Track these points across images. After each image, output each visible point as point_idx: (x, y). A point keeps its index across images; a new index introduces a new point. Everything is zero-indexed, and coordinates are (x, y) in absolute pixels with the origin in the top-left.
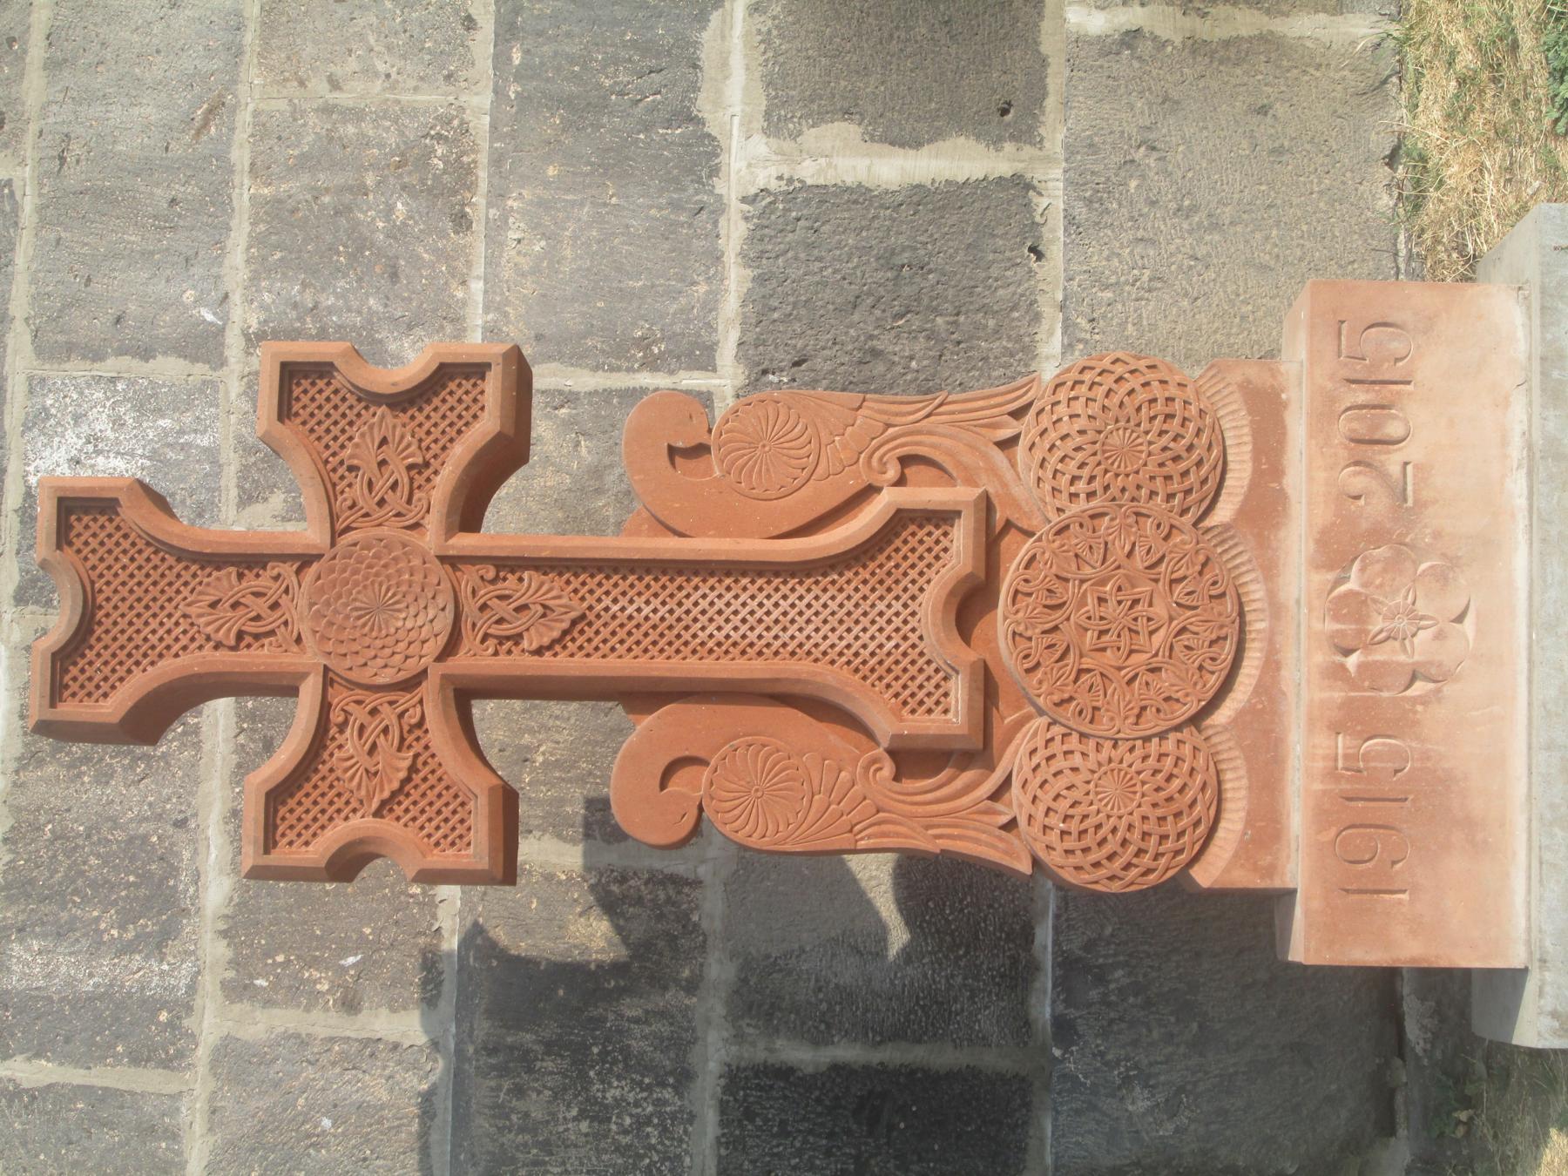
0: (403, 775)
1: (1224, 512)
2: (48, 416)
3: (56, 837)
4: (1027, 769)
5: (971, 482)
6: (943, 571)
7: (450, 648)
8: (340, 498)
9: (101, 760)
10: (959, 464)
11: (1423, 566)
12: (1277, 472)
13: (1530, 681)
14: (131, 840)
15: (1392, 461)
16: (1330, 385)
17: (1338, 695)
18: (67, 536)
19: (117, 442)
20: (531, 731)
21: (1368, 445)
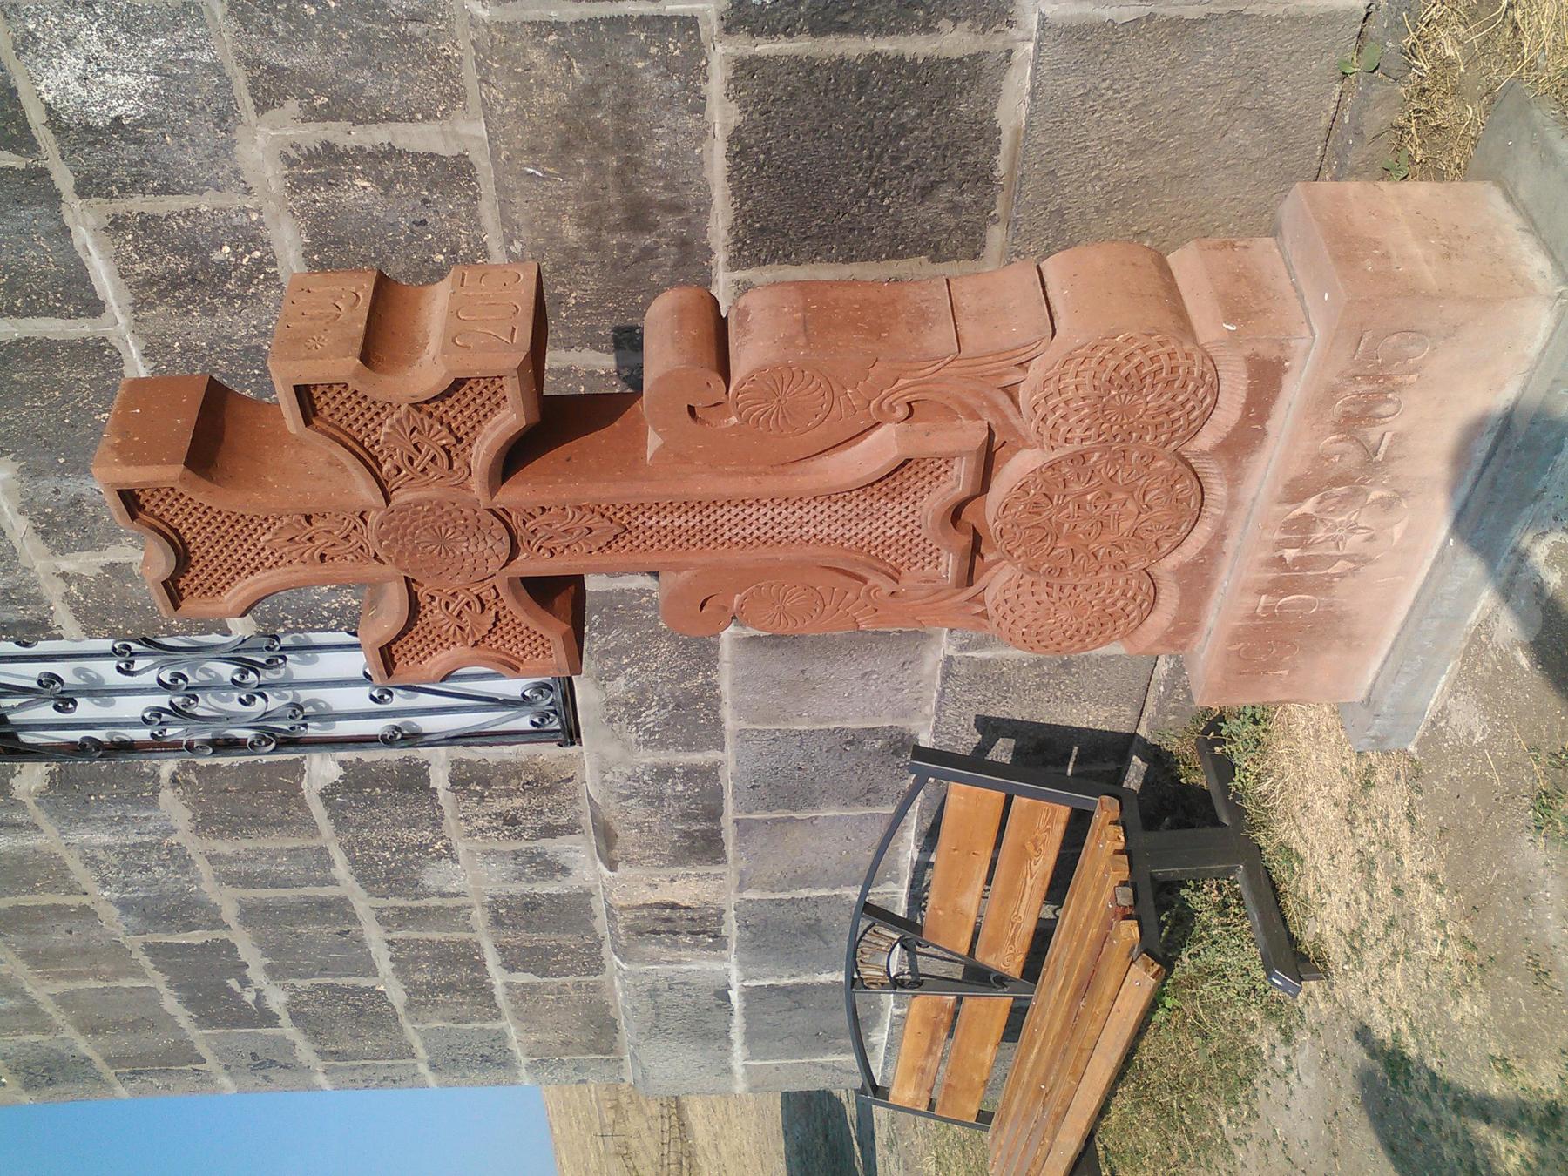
0: (490, 627)
1: (1206, 440)
2: (36, 41)
3: (184, 351)
4: (1000, 598)
5: (974, 415)
6: (944, 488)
7: (513, 555)
8: (385, 467)
9: (203, 301)
10: (964, 405)
11: (1375, 494)
12: (1262, 418)
13: (1436, 563)
14: (247, 349)
15: (1373, 435)
16: (1337, 380)
17: (1271, 576)
18: (137, 503)
19: (117, 61)
20: (562, 284)
21: (1354, 422)
